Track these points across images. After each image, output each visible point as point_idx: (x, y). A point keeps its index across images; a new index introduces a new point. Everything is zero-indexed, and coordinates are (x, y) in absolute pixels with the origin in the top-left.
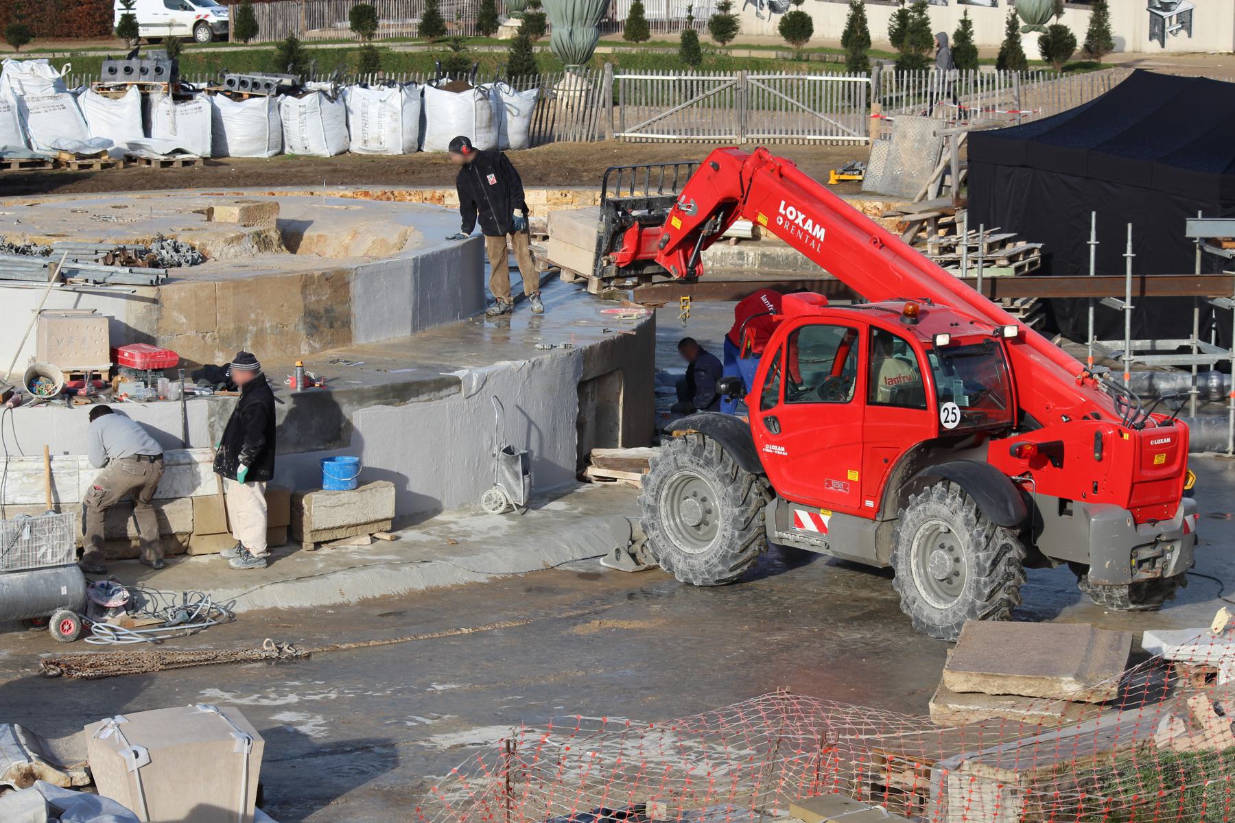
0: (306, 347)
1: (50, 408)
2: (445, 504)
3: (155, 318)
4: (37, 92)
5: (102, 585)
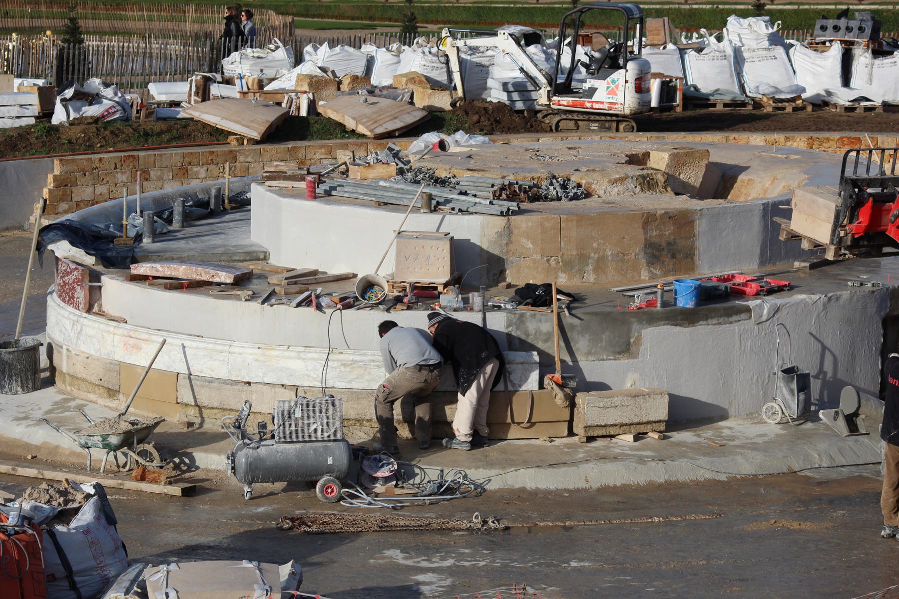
0: (646, 273)
1: (372, 311)
2: (732, 412)
3: (504, 242)
4: (754, 44)
5: (375, 459)
